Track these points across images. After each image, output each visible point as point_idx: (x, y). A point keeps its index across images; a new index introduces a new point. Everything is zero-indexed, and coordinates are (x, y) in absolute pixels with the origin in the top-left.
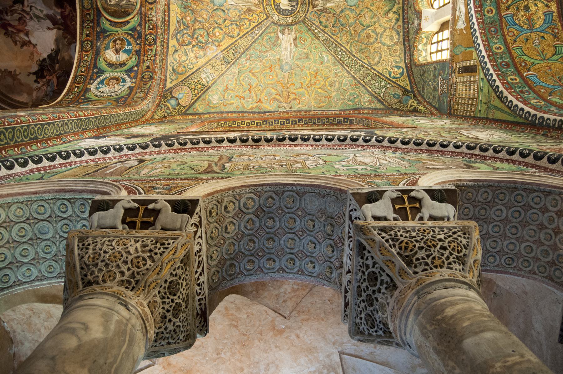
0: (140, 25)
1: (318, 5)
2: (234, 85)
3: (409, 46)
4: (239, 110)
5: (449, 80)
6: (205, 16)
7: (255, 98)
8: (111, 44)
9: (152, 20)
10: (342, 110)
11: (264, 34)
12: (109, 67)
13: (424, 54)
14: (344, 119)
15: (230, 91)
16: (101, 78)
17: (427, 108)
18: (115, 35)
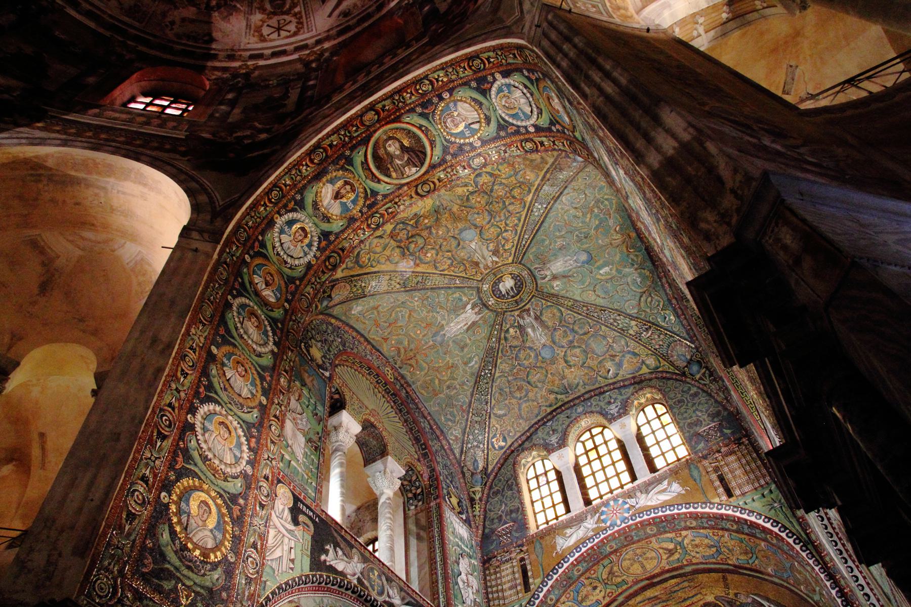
0: (385, 196)
1: (523, 319)
2: (385, 310)
3: (531, 435)
4: (363, 332)
5: (511, 543)
6: (441, 233)
7: (386, 334)
8: (340, 183)
9: (399, 206)
10: (431, 416)
11: (461, 290)
12: (313, 205)
13: (530, 459)
14: (424, 444)
15: (375, 312)
16: (295, 216)
17: (479, 516)
18: (355, 177)
